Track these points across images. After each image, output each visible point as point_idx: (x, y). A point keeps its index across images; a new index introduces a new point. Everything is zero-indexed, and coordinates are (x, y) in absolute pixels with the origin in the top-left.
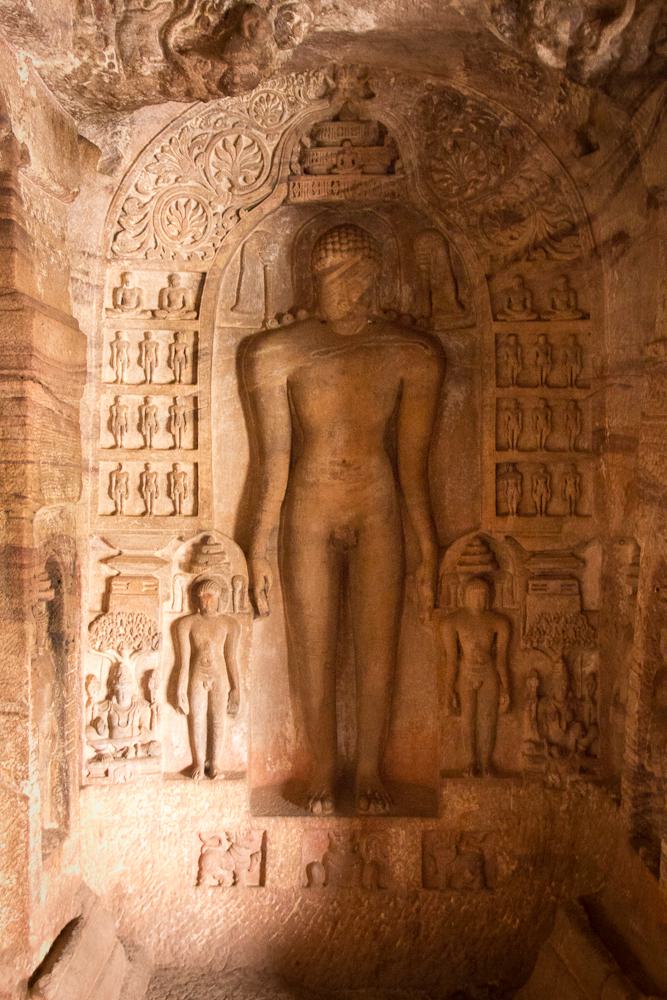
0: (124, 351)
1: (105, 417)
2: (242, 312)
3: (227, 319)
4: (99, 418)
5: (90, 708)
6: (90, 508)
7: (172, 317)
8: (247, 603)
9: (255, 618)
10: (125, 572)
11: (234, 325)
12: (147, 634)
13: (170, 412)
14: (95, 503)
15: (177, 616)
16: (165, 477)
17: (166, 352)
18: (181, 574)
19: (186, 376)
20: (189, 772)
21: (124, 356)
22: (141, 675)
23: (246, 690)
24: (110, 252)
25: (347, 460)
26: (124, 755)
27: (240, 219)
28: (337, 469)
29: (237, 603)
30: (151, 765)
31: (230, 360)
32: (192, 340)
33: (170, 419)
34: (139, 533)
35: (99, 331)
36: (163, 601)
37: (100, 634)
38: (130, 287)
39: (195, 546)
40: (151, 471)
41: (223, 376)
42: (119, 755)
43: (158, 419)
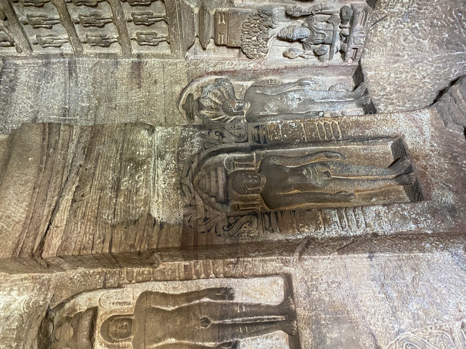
1: (99, 50)
4: (100, 54)
5: (306, 56)
6: (167, 60)
10: (211, 34)
12: (258, 21)
13: (81, 5)
14: (163, 56)
16: (134, 8)
22: (289, 19)
26: (346, 36)
30: (359, 18)
33: (84, 5)
35: (36, 57)
37: (256, 52)
42: (344, 38)
43: (88, 13)
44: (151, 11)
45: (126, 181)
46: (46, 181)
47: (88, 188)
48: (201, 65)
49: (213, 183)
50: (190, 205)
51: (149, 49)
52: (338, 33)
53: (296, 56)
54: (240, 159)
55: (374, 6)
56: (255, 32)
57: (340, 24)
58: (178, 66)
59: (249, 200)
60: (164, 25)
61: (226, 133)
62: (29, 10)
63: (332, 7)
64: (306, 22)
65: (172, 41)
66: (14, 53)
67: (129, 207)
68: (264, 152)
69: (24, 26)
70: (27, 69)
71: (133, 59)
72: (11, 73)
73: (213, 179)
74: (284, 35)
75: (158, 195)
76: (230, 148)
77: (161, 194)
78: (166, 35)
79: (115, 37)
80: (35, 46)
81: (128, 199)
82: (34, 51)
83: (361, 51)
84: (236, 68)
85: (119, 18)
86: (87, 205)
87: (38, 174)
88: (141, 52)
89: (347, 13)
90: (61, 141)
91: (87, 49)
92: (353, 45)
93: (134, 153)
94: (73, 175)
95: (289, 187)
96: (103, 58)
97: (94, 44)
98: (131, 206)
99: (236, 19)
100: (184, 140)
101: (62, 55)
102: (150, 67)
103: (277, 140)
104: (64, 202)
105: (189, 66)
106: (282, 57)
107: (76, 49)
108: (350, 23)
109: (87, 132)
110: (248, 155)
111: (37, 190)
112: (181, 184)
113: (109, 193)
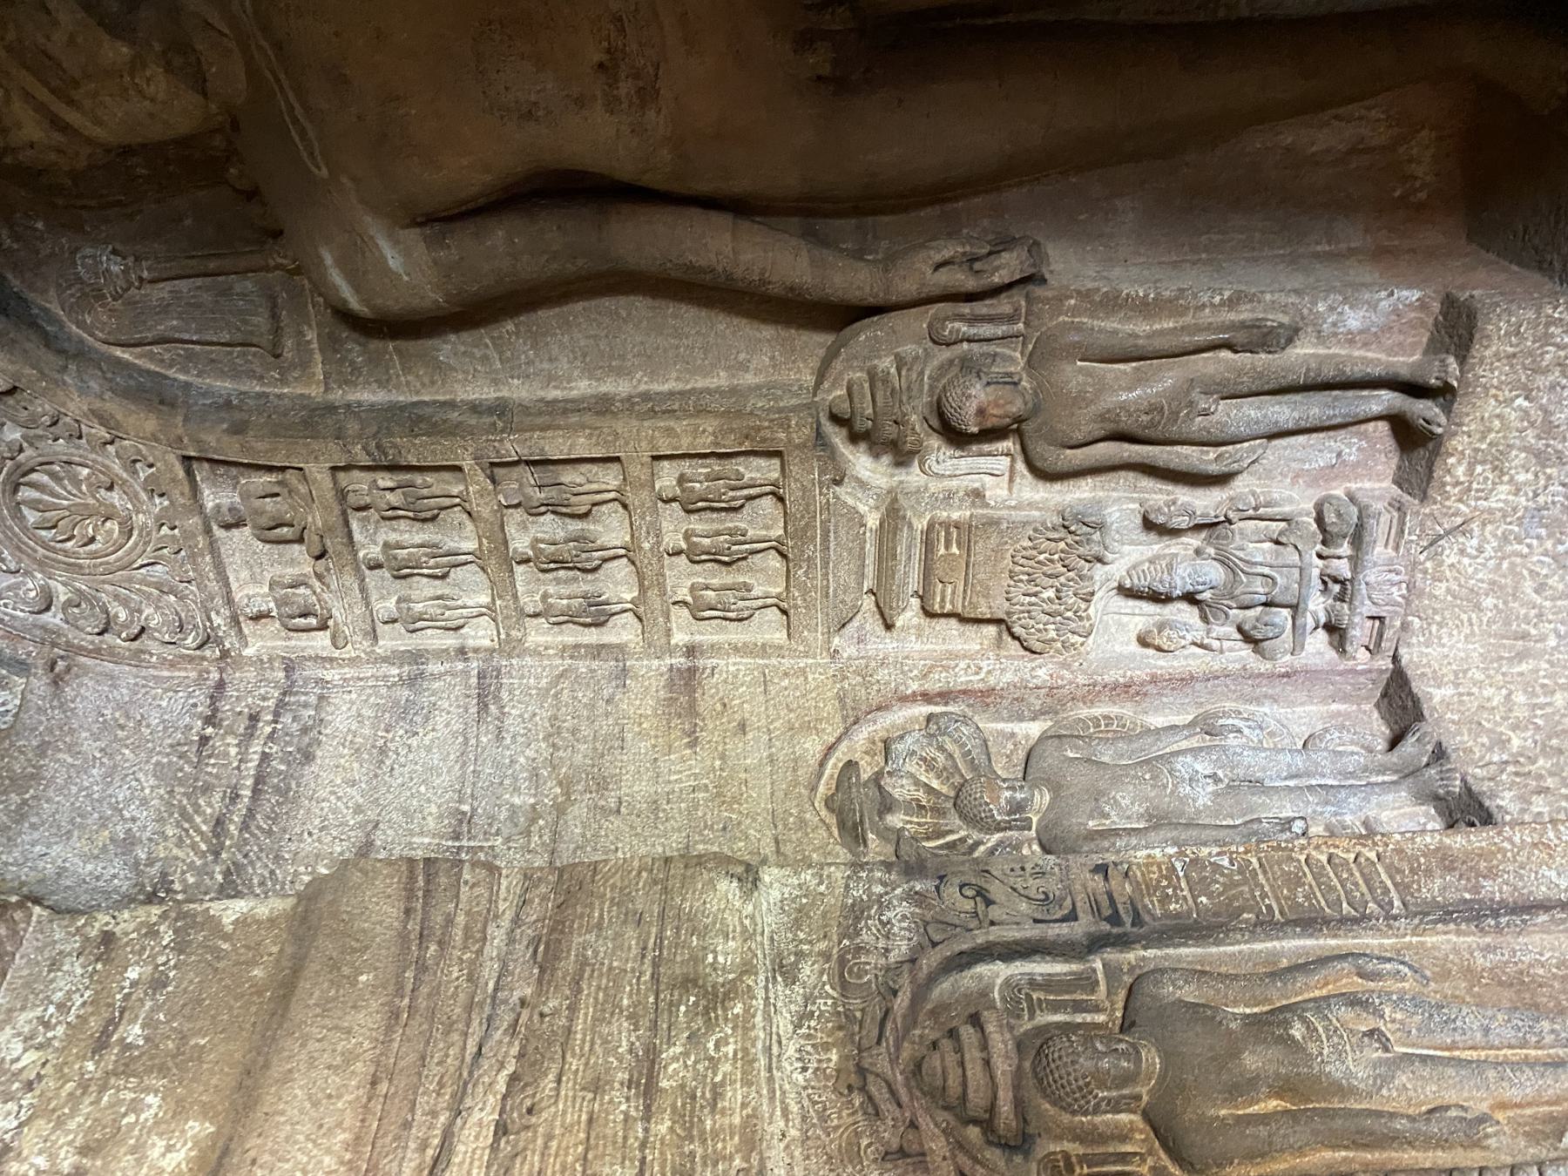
0: (418, 607)
1: (573, 635)
2: (277, 331)
3: (305, 365)
4: (577, 646)
5: (1216, 644)
6: (774, 661)
7: (316, 519)
8: (1003, 305)
9: (1044, 281)
10: (914, 582)
11: (315, 345)
12: (1062, 545)
14: (764, 650)
15: (1021, 466)
17: (403, 524)
18: (922, 464)
19: (449, 483)
20: (1410, 437)
21: (433, 608)
22: (1153, 536)
23: (1231, 303)
24: (208, 653)
25: (598, 57)
26: (1342, 583)
27: (15, 388)
28: (625, 88)
29: (1001, 330)
30: (1380, 529)
31: (397, 350)
32: (356, 474)
33: (554, 512)
34: (826, 564)
35: (385, 660)
36: (987, 506)
37: (1053, 634)
38: (272, 605)
39: (854, 438)
40: (684, 546)
41: (438, 367)
42: (1337, 588)
44: (742, 525)
45: (675, 1059)
46: (413, 1057)
47: (549, 1083)
48: (882, 674)
49: (975, 1072)
50: (902, 1153)
51: (722, 630)
52: (1316, 572)
53: (1183, 642)
54: (1049, 984)
55: (1425, 493)
56: (1049, 576)
57: (1319, 547)
58: (810, 677)
59: (1103, 1139)
60: (774, 561)
61: (996, 890)
62: (394, 530)
63: (1290, 500)
64: (1209, 543)
65: (796, 607)
66: (324, 648)
67: (692, 1154)
68: (1131, 956)
69: (367, 572)
70: (354, 696)
71: (673, 661)
72: (306, 705)
73: (973, 1055)
74: (1142, 583)
75: (785, 1112)
76: (1016, 942)
77: (794, 1108)
78: (779, 590)
79: (628, 597)
80: (386, 627)
81: (688, 1126)
82: (381, 643)
83: (1398, 623)
84: (992, 681)
85: (646, 546)
86: (546, 1146)
87: (389, 1030)
88: (698, 638)
89: (1339, 515)
90: (461, 919)
91: (538, 635)
92: (1367, 609)
93: (696, 960)
94: (498, 1035)
95: (1242, 1088)
96: (581, 658)
97: (562, 619)
98: (700, 1151)
99: (994, 541)
100: (856, 913)
101: (462, 652)
102: (725, 681)
103: (1178, 915)
104: (469, 1133)
105: (845, 678)
106: (1135, 647)
107: (508, 635)
108: (1352, 543)
109: (543, 889)
110: (1074, 967)
111: (383, 1087)
112: (862, 1071)
113: (621, 1103)
